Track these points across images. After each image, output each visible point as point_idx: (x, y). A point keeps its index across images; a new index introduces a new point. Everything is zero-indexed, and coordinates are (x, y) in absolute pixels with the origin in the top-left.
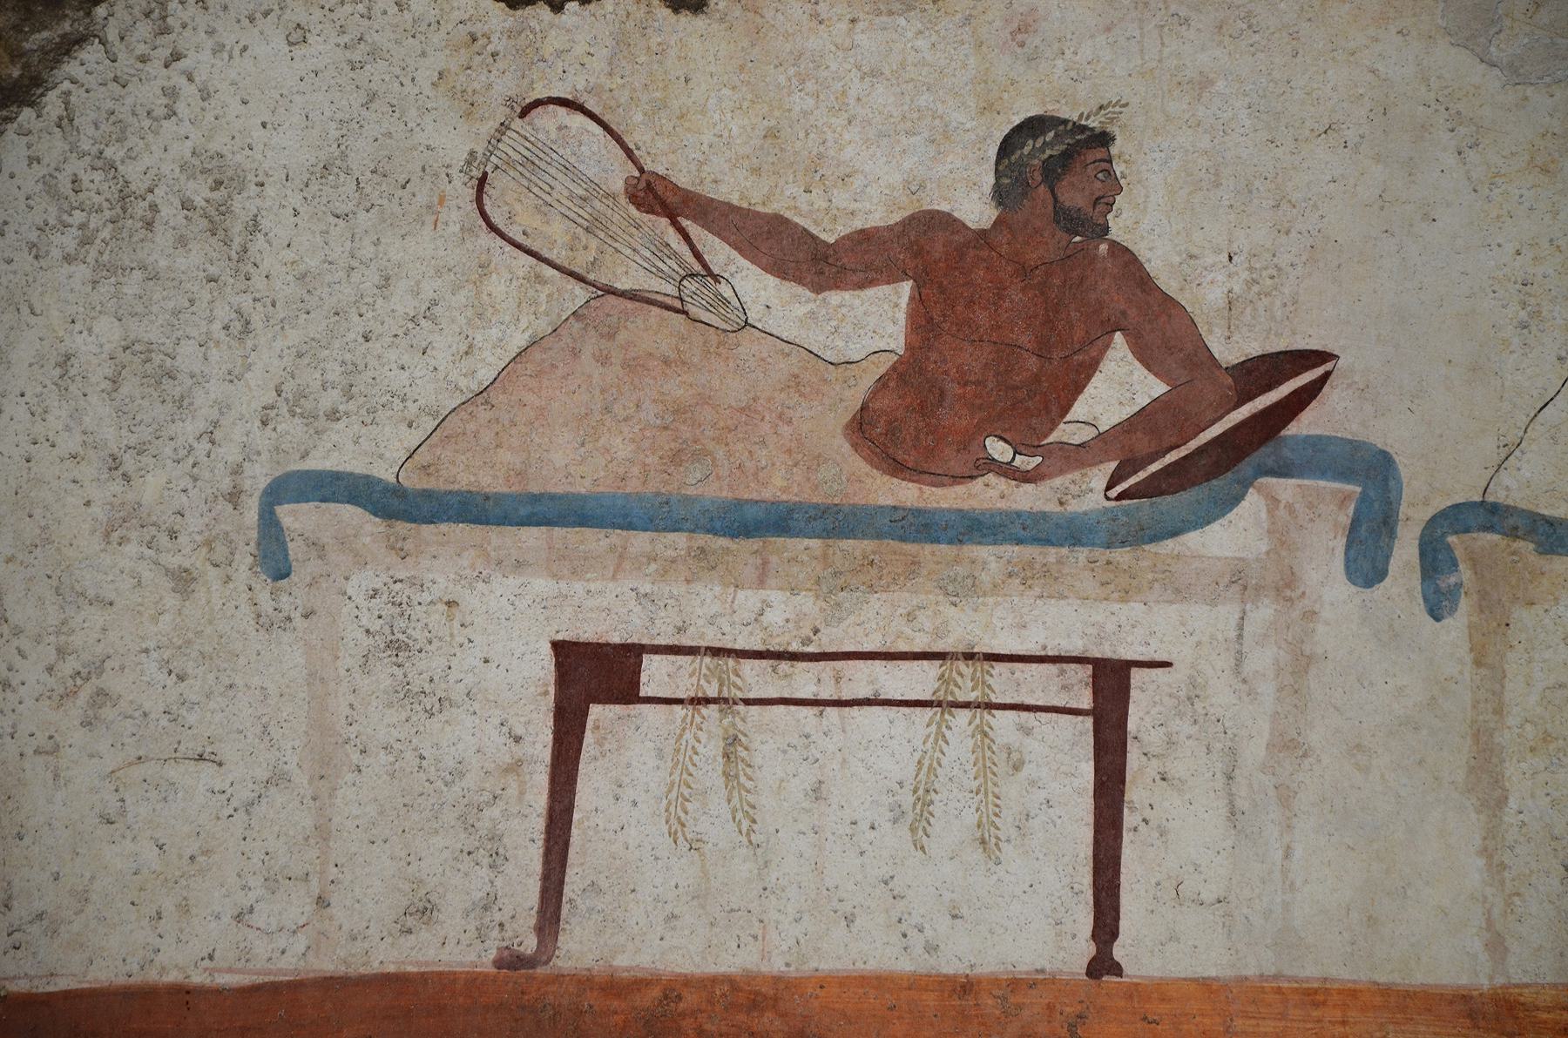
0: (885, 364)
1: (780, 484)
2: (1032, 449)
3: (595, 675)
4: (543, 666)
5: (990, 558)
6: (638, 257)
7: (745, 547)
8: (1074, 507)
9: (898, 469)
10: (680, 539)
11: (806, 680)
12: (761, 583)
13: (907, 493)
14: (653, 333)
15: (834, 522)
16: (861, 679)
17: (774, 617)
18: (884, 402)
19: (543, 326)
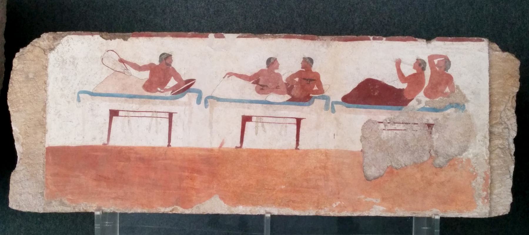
0: (146, 80)
1: (135, 93)
2: (163, 89)
3: (114, 113)
4: (108, 113)
5: (158, 101)
6: (120, 67)
7: (130, 100)
8: (167, 96)
9: (148, 91)
10: (123, 98)
11: (137, 114)
12: (133, 103)
13: (149, 94)
14: (121, 76)
15: (141, 97)
16: (143, 114)
17: (134, 107)
18: (147, 84)
19: (109, 75)
